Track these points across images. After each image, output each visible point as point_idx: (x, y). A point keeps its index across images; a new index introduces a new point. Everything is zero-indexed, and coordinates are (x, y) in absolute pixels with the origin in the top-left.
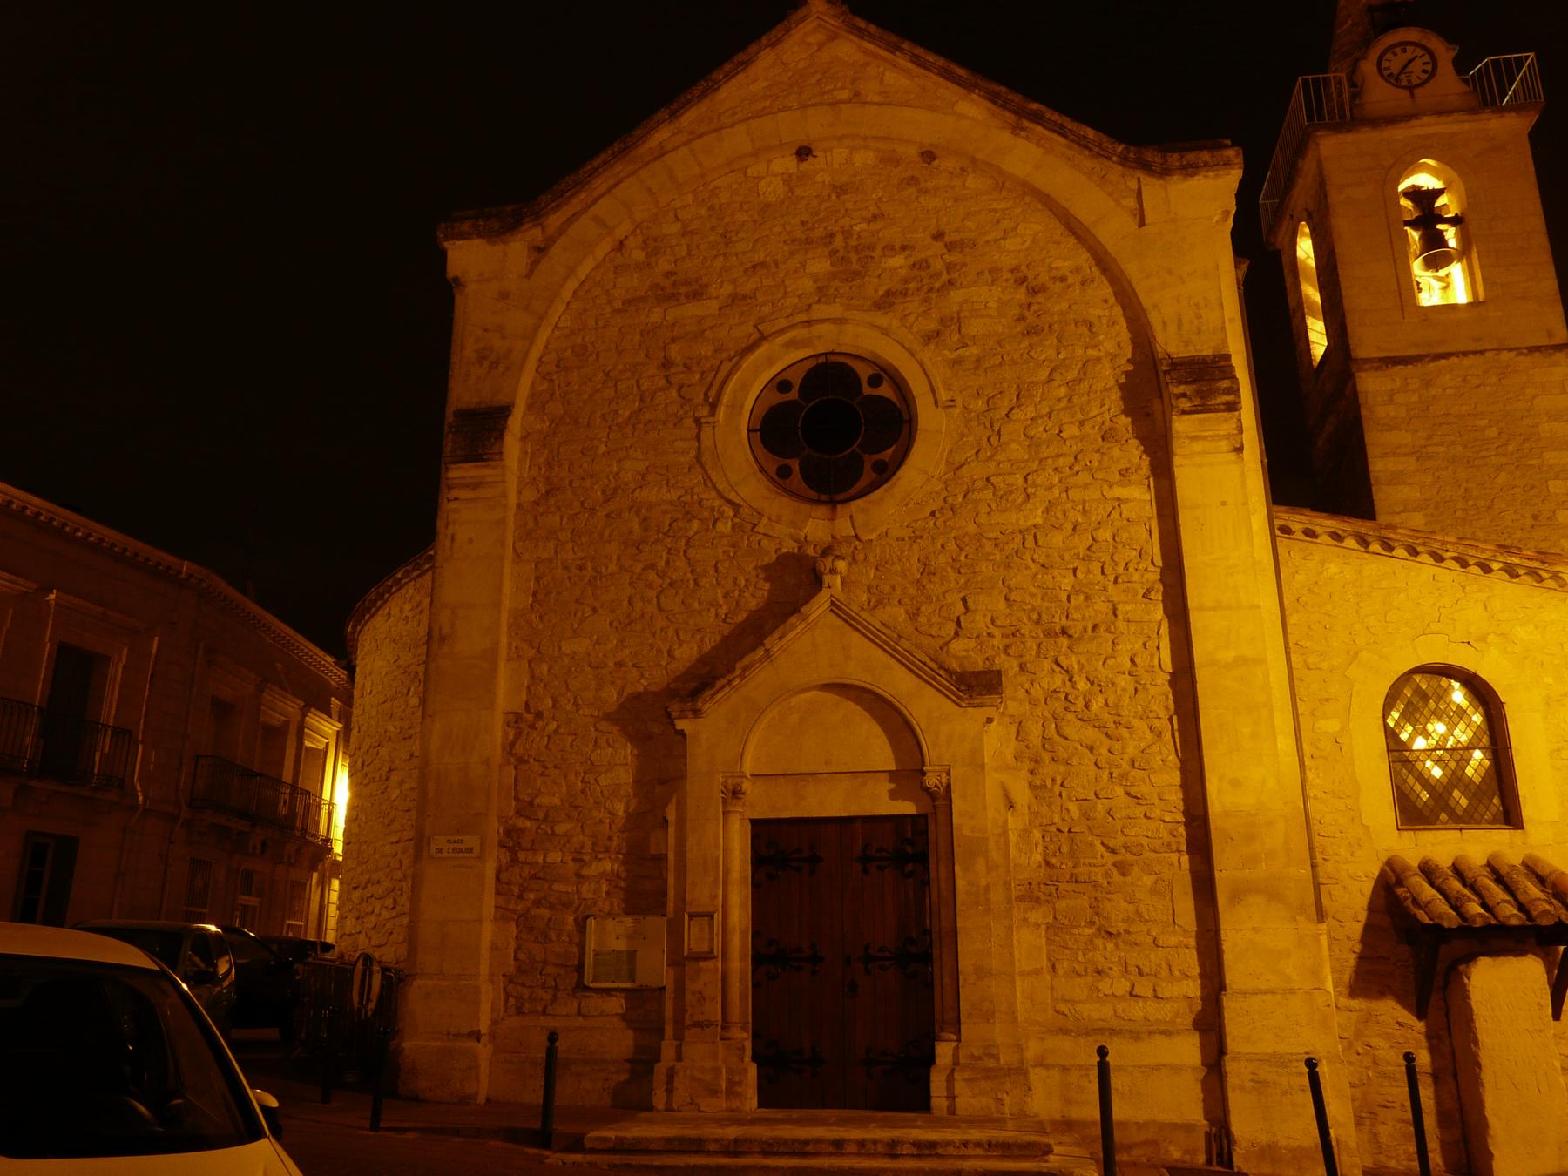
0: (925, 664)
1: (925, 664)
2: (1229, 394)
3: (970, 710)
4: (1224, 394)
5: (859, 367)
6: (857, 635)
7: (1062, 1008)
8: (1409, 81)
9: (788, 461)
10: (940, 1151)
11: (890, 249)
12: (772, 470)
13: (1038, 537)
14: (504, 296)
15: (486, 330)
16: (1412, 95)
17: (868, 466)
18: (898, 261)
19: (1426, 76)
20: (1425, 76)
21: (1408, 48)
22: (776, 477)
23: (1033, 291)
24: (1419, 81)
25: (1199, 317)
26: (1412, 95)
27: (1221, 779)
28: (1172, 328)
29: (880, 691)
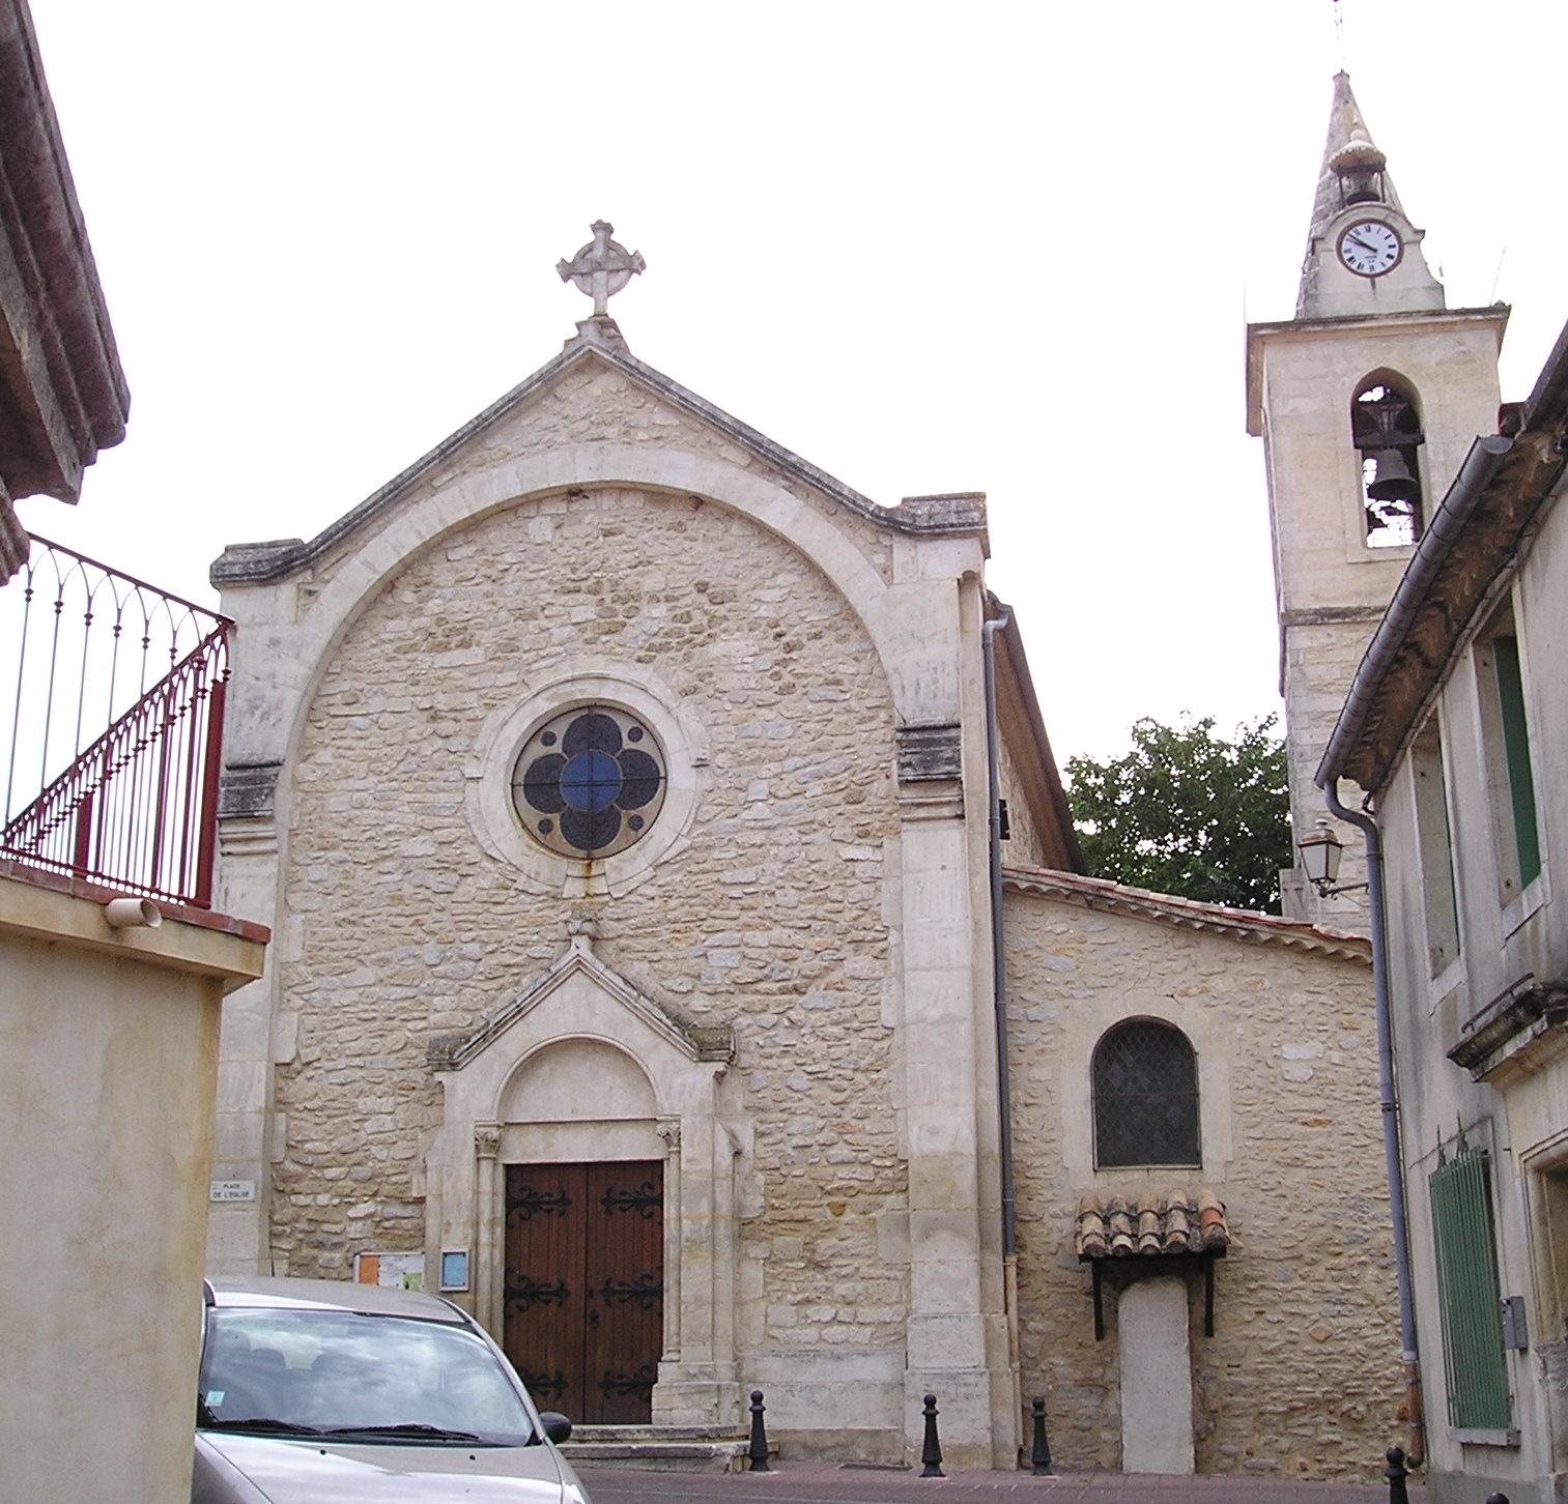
0: (661, 1020)
1: (661, 1020)
2: (950, 764)
3: (701, 1064)
4: (946, 764)
5: (620, 720)
6: (601, 992)
7: (774, 1332)
8: (1372, 268)
9: (549, 816)
10: (618, 1436)
11: (654, 599)
12: (534, 825)
13: (849, 857)
14: (274, 643)
15: (257, 679)
16: (1373, 284)
17: (624, 822)
18: (661, 610)
19: (1392, 262)
20: (1390, 262)
21: (1372, 226)
22: (537, 833)
23: (789, 648)
24: (1383, 269)
25: (936, 681)
26: (1373, 284)
27: (920, 1128)
28: (910, 693)
29: (622, 1047)
